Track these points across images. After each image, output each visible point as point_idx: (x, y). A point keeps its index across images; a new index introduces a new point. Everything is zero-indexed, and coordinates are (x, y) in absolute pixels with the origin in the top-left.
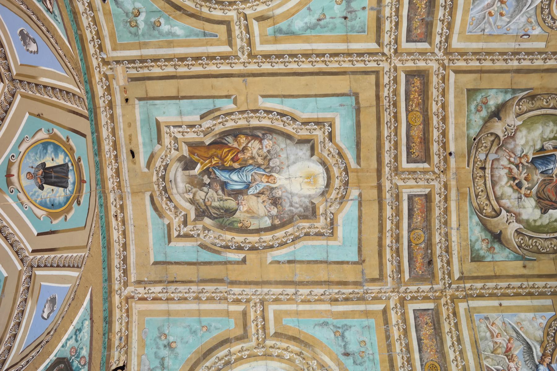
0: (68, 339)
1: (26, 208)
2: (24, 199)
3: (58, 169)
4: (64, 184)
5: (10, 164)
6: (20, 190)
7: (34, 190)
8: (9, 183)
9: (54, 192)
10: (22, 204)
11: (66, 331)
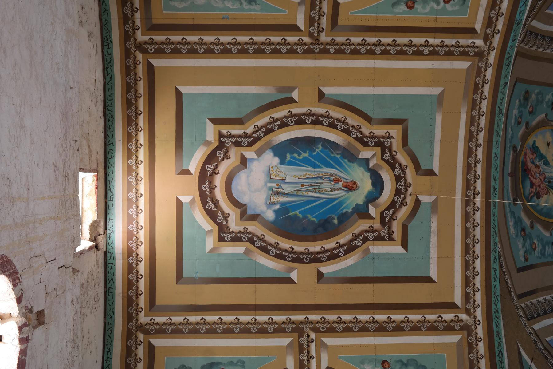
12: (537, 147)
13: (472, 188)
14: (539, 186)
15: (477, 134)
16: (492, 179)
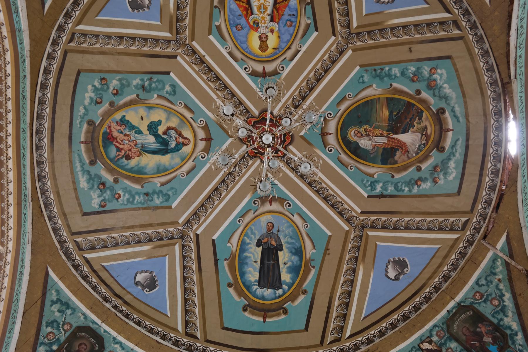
0: (121, 344)
1: (239, 222)
2: (247, 219)
3: (277, 272)
4: (262, 282)
5: (282, 200)
6: (256, 213)
7: (256, 232)
8: (263, 200)
9: (255, 264)
10: (243, 216)
11: (128, 339)
12: (128, 121)
13: (5, 154)
14: (130, 150)
15: (6, 115)
16: (22, 148)
